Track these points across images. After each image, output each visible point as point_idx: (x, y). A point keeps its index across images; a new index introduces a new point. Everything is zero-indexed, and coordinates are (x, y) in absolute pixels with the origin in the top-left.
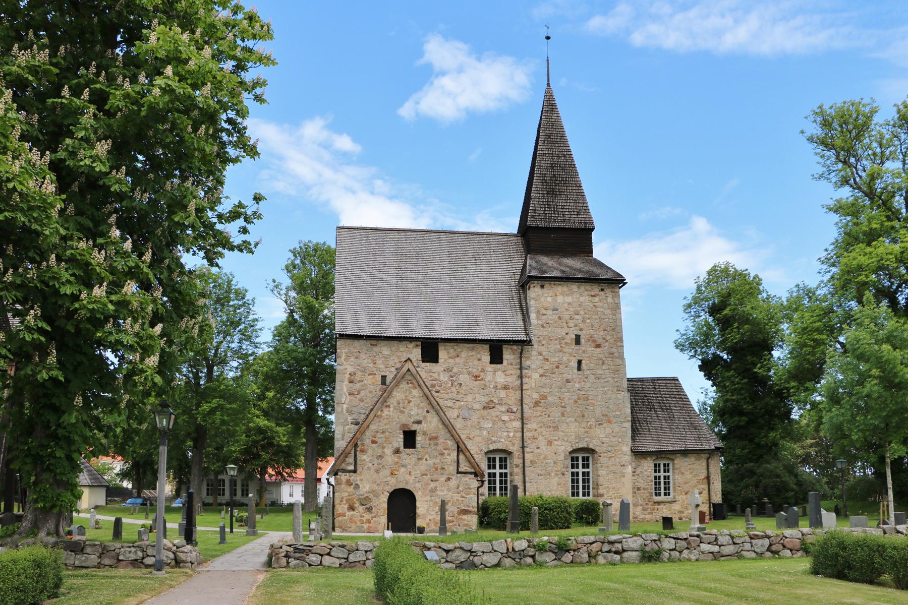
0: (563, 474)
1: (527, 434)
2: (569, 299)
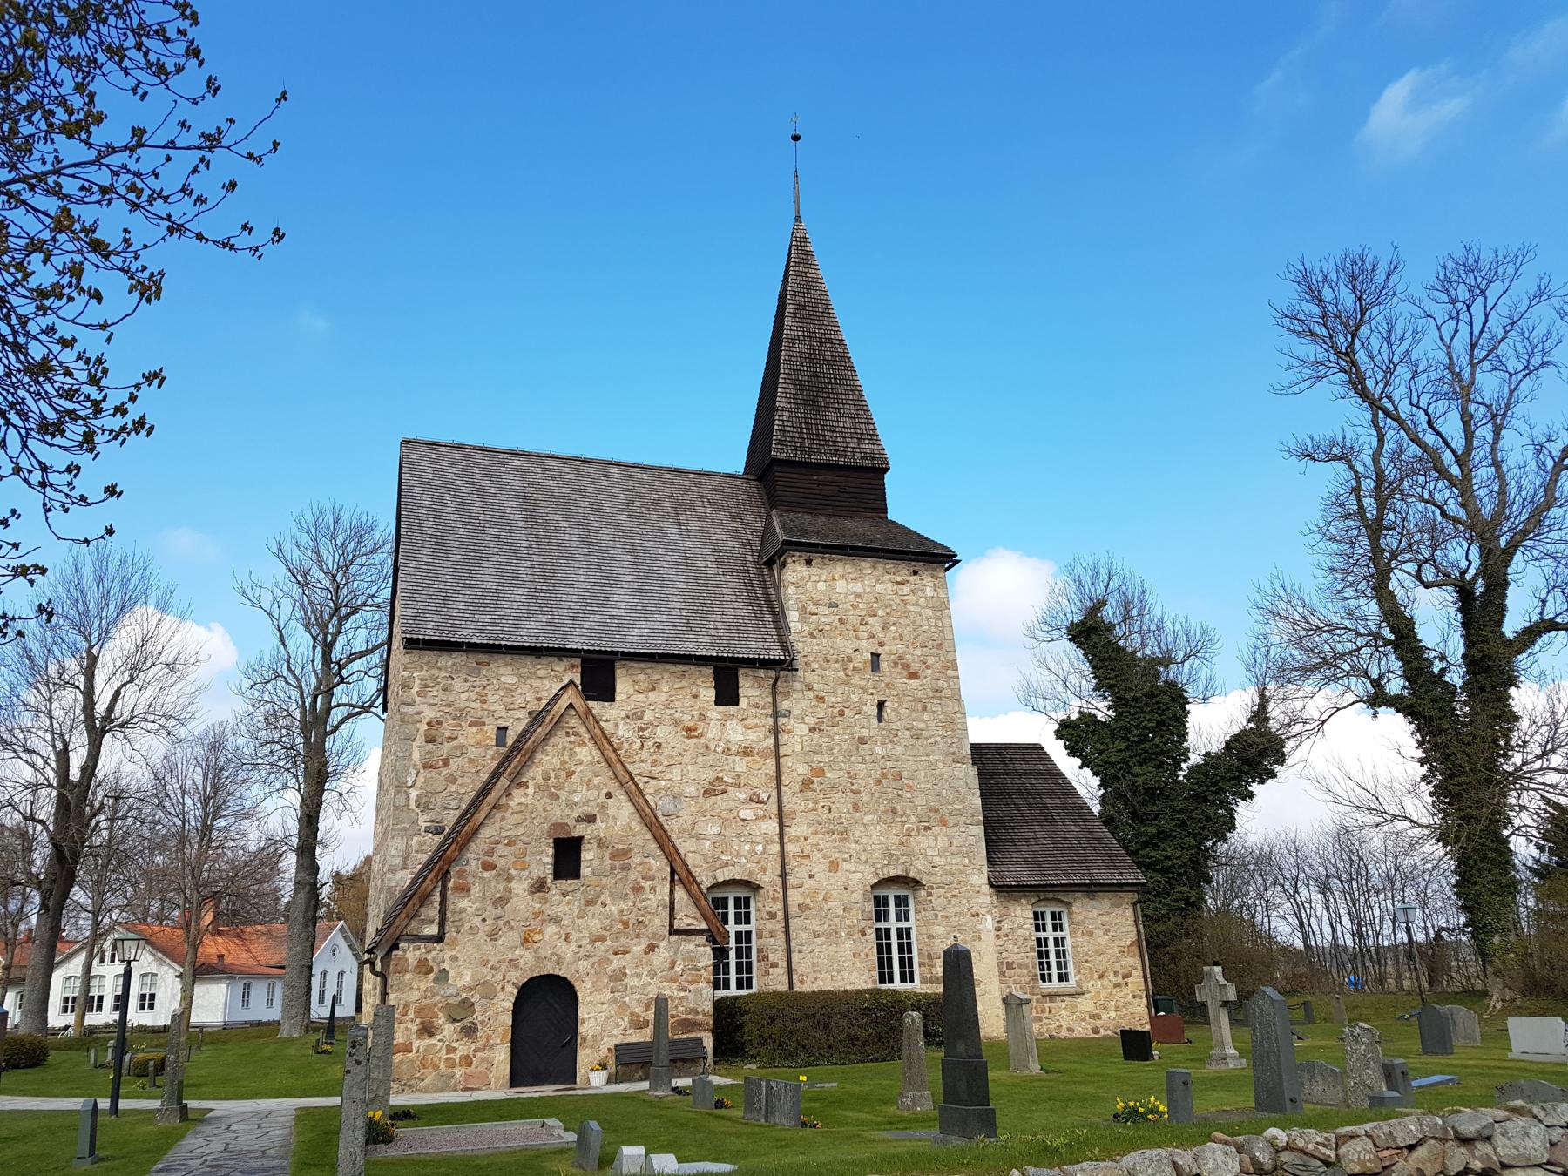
0: (864, 934)
1: (791, 849)
2: (858, 587)
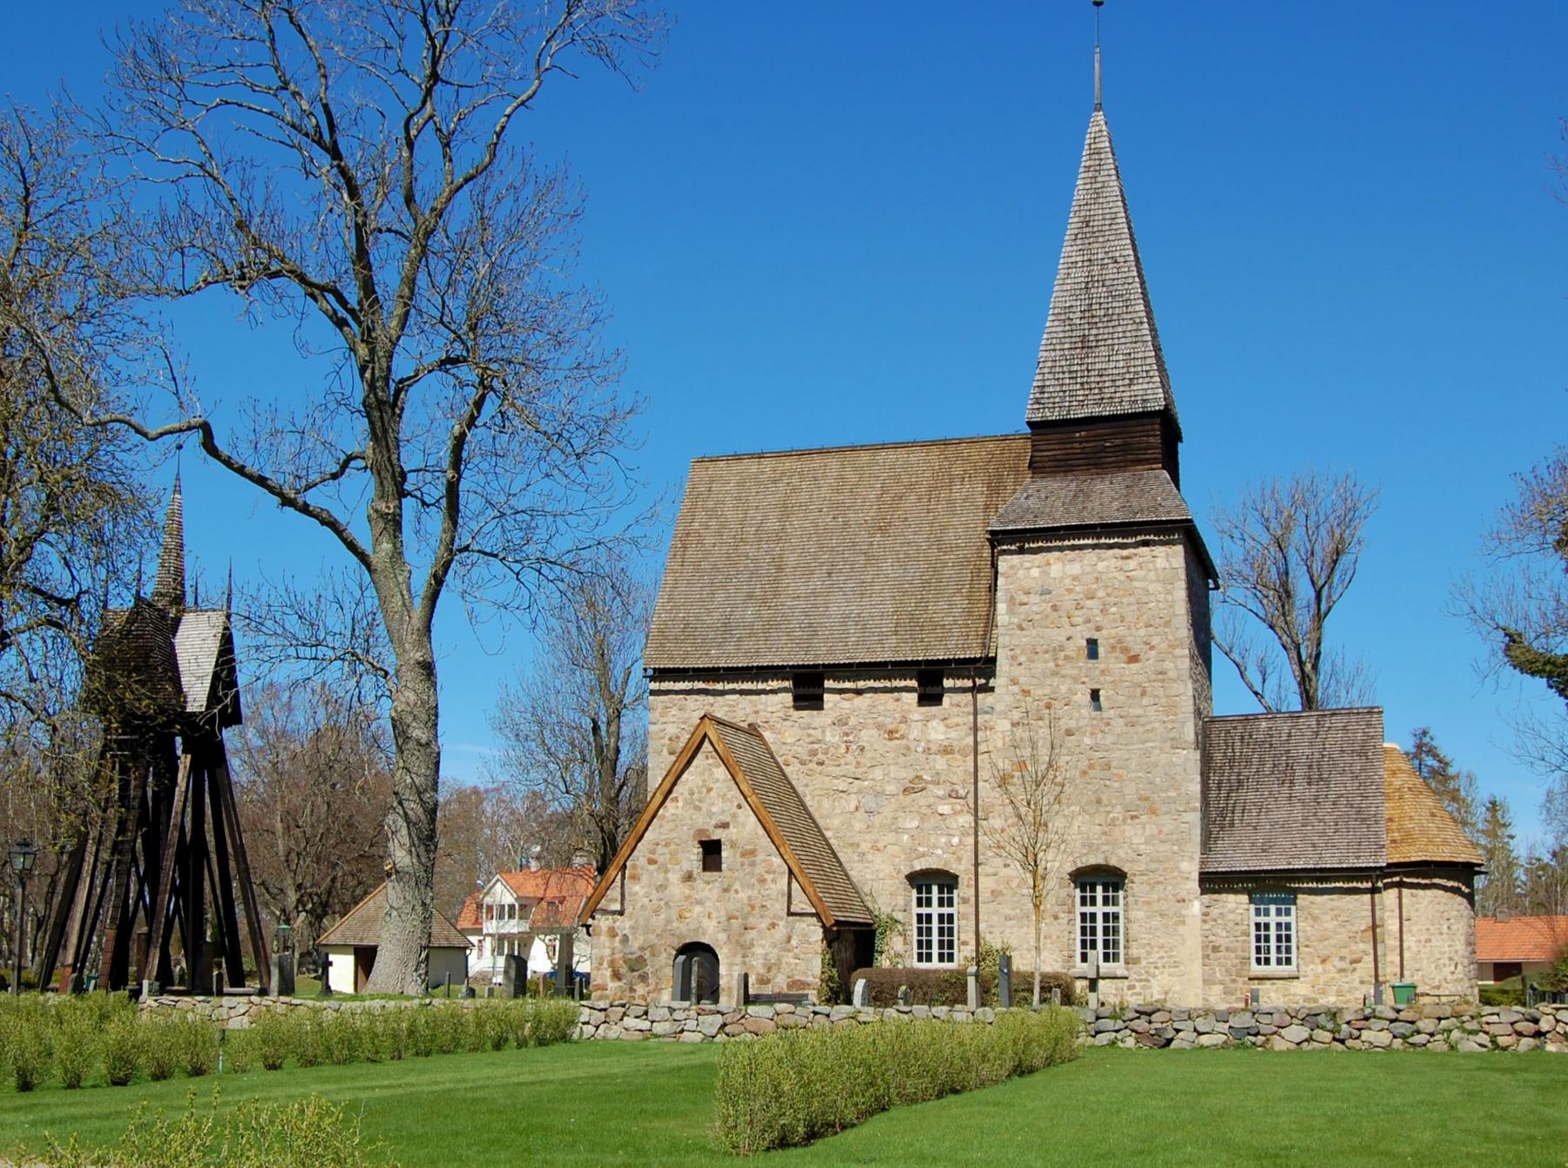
0: (1056, 918)
2: (1075, 569)
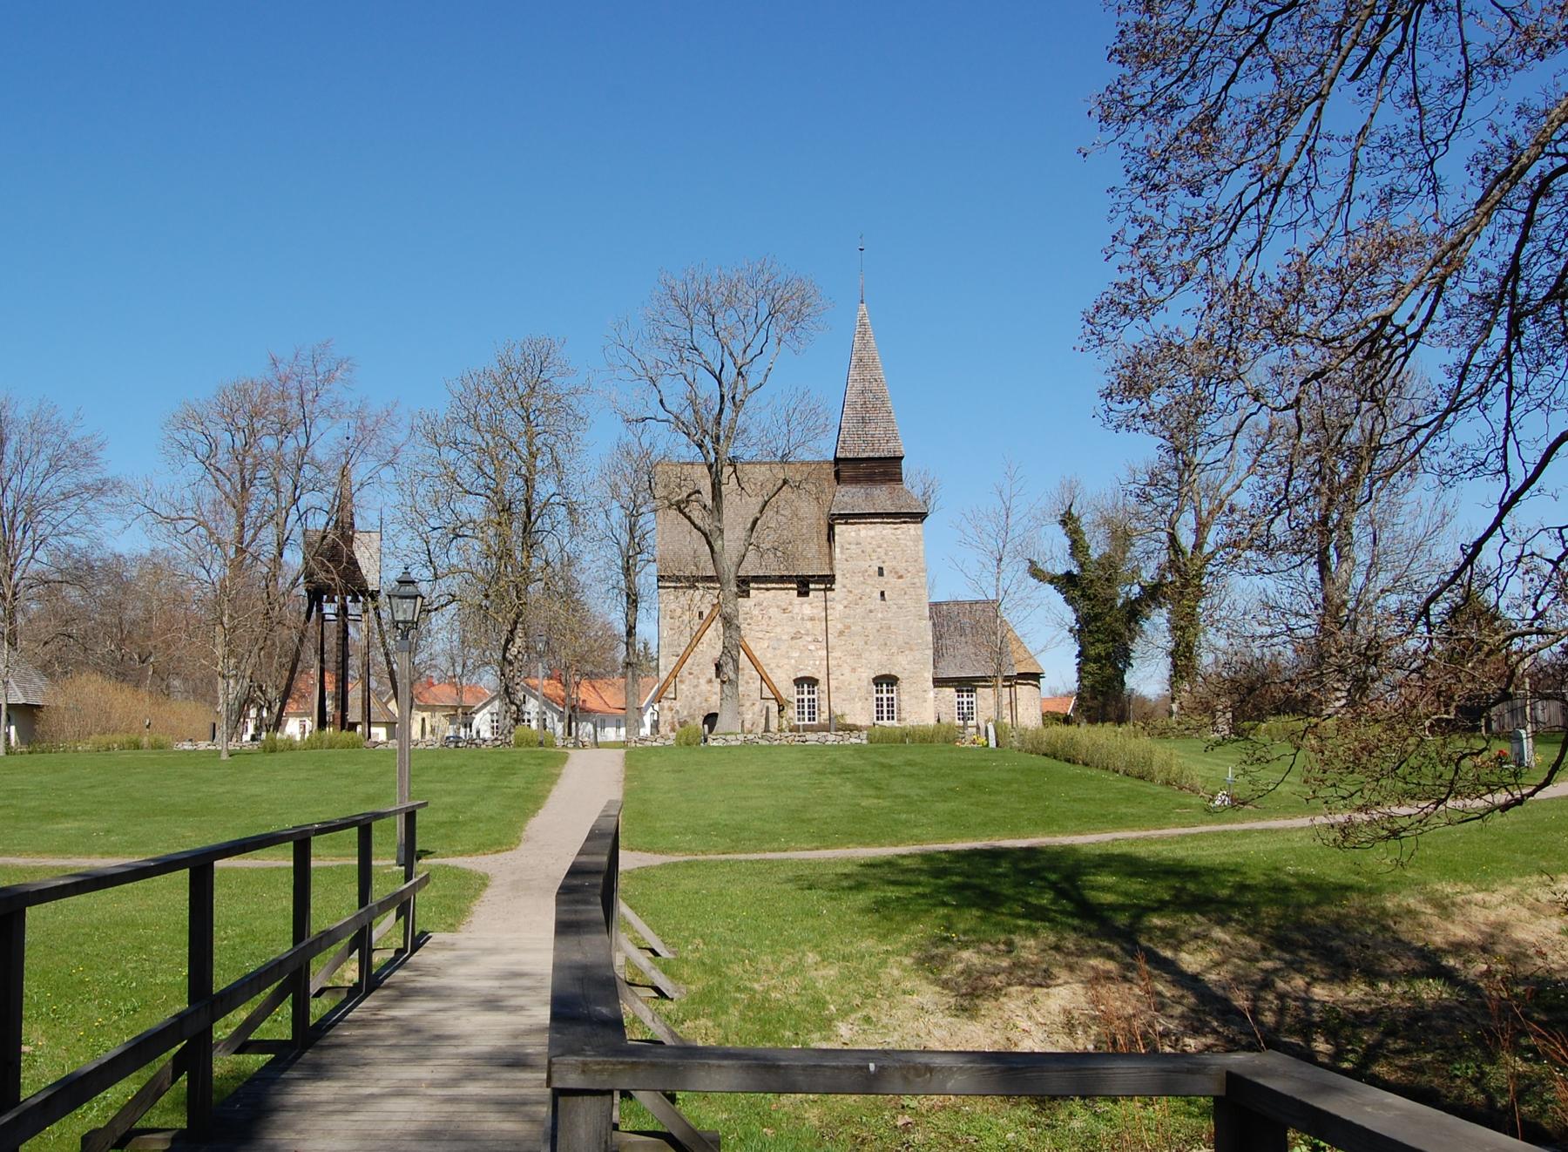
2: (872, 533)
